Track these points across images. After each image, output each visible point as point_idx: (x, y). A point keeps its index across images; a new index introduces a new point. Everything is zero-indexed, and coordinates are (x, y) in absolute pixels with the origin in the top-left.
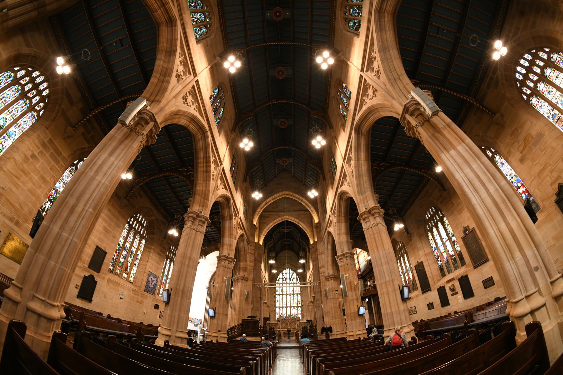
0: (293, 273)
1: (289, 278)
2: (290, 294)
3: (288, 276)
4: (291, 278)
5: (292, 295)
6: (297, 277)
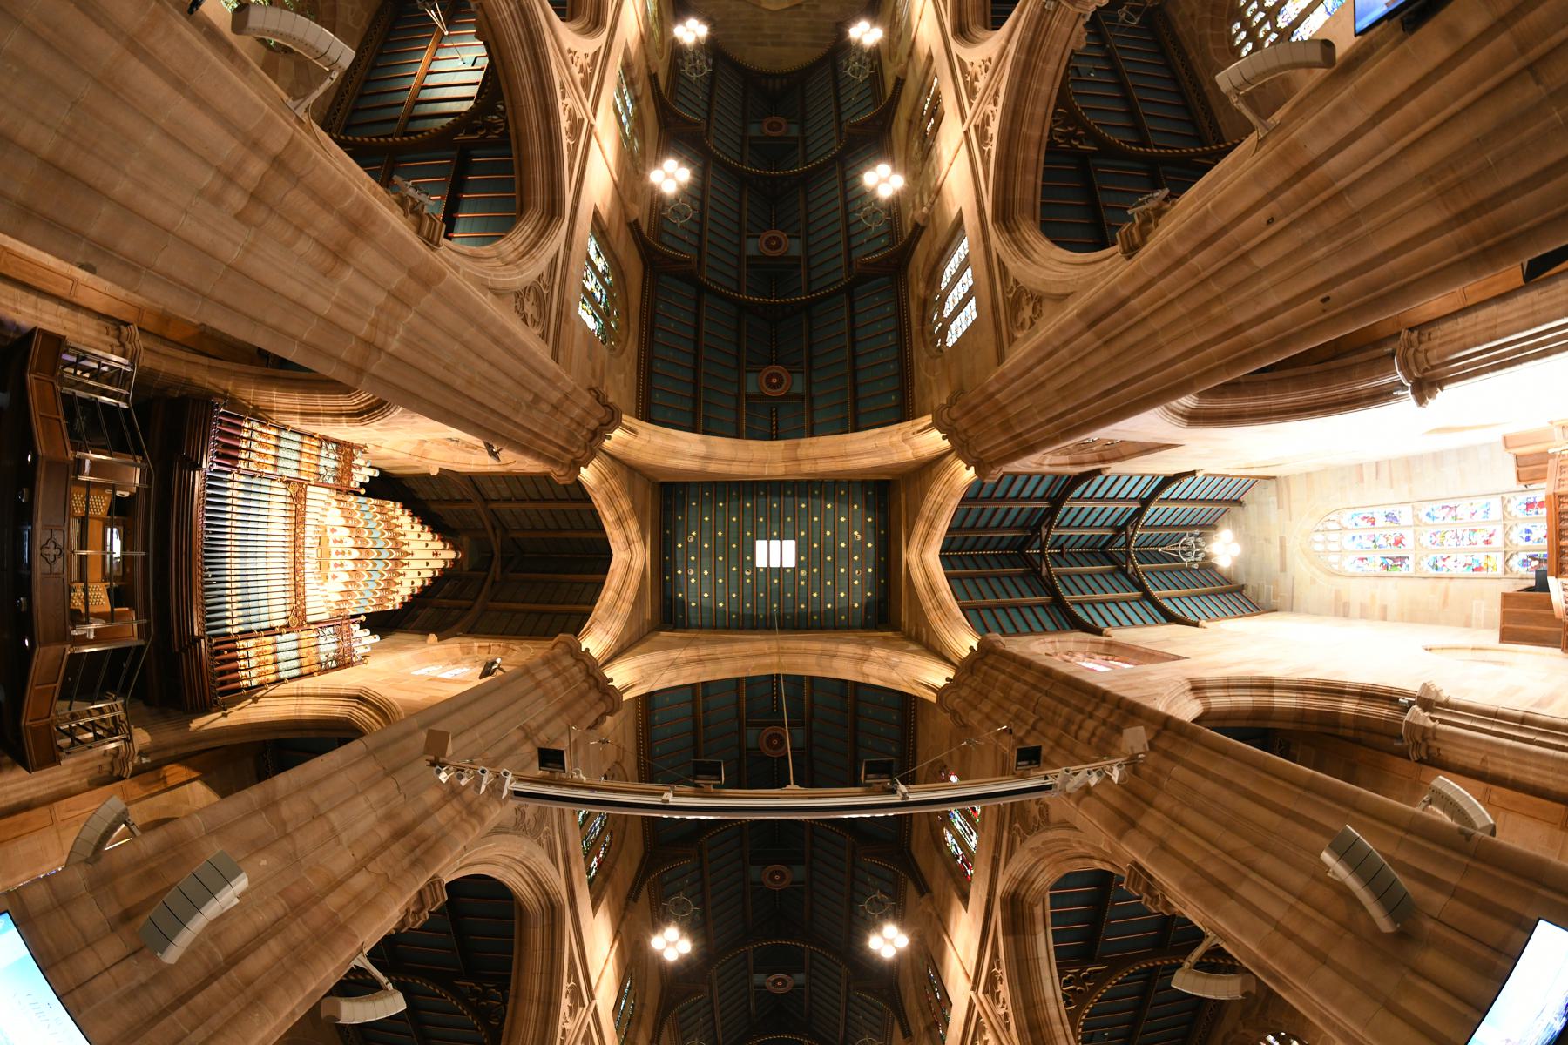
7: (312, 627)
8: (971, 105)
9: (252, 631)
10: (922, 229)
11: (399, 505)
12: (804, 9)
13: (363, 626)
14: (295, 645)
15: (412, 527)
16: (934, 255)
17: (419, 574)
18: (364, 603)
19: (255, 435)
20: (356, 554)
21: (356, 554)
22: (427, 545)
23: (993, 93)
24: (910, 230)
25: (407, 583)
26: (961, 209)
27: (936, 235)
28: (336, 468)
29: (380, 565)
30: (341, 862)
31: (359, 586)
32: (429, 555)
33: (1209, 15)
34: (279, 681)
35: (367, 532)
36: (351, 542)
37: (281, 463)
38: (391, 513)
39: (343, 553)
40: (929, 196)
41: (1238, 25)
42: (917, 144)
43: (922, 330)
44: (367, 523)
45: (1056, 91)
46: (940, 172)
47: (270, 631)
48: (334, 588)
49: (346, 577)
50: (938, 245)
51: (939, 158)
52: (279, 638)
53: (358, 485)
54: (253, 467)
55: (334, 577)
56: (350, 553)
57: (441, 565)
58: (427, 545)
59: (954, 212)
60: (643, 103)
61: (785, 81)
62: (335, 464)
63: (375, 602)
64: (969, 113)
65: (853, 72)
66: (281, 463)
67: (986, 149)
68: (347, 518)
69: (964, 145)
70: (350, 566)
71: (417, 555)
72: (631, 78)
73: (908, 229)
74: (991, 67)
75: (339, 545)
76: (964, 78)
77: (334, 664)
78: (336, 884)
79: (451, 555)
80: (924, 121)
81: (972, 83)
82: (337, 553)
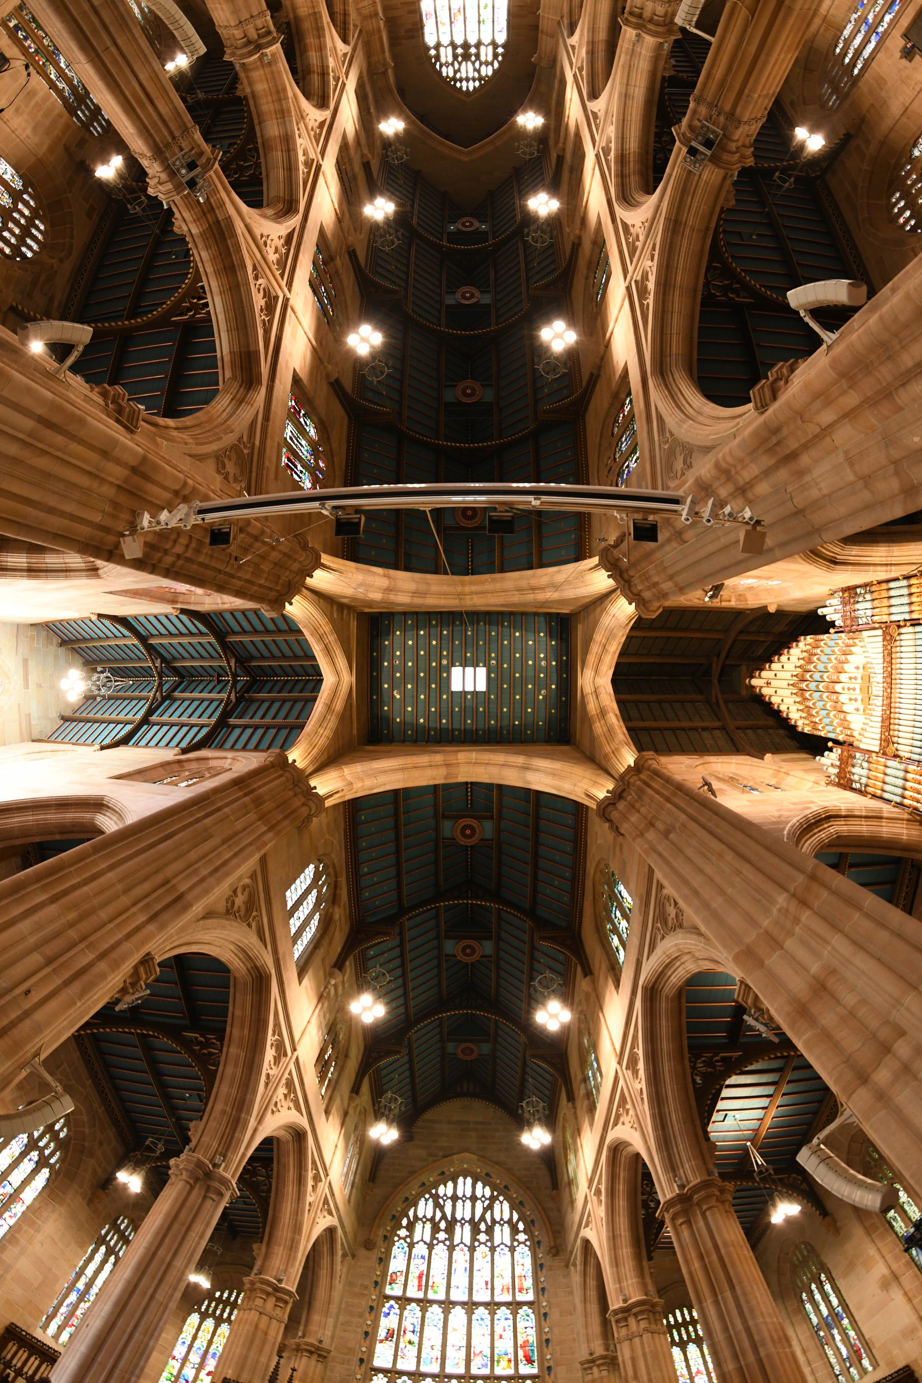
0: (493, 1199)
1: (472, 1221)
2: (470, 1306)
3: (463, 1211)
4: (483, 1218)
5: (481, 1312)
6: (516, 1217)
7: (877, 625)
8: (290, 1073)
10: (335, 966)
11: (800, 729)
12: (441, 1153)
13: (832, 624)
14: (893, 610)
16: (325, 943)
17: (783, 667)
18: (832, 643)
20: (838, 688)
21: (838, 688)
23: (270, 1084)
24: (347, 963)
25: (794, 659)
26: (300, 983)
27: (323, 960)
28: (853, 766)
29: (817, 676)
30: (845, 435)
31: (836, 659)
32: (774, 683)
33: (87, 1144)
34: (907, 578)
35: (828, 706)
36: (842, 698)
38: (807, 722)
39: (849, 689)
40: (329, 993)
41: (62, 1135)
42: (341, 1037)
43: (336, 877)
44: (828, 714)
45: (216, 1085)
46: (319, 1015)
48: (857, 659)
49: (846, 666)
50: (321, 952)
51: (320, 1027)
52: (907, 617)
53: (834, 750)
55: (857, 668)
56: (843, 689)
57: (764, 674)
59: (306, 981)
60: (580, 1077)
61: (459, 1090)
62: (854, 770)
63: (822, 643)
64: (292, 1066)
65: (396, 1099)
67: (276, 1037)
68: (845, 720)
69: (296, 1039)
70: (843, 677)
71: (784, 684)
72: (589, 1099)
73: (349, 964)
74: (272, 1106)
75: (853, 697)
76: (296, 1096)
77: (858, 590)
78: (849, 415)
79: (755, 682)
80: (334, 1057)
81: (289, 1092)
82: (854, 689)
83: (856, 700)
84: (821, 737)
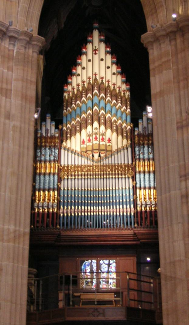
9: (134, 200)
15: (79, 75)
17: (108, 67)
18: (124, 118)
19: (41, 204)
20: (96, 124)
21: (96, 124)
22: (90, 61)
28: (50, 148)
32: (96, 57)
36: (89, 128)
37: (52, 187)
38: (71, 95)
47: (135, 188)
49: (109, 131)
52: (138, 185)
54: (55, 204)
55: (109, 141)
56: (96, 129)
57: (103, 45)
58: (90, 61)
66: (52, 187)
70: (103, 128)
71: (96, 71)
79: (96, 33)
82: (96, 138)
83: (89, 140)
84: (63, 110)
